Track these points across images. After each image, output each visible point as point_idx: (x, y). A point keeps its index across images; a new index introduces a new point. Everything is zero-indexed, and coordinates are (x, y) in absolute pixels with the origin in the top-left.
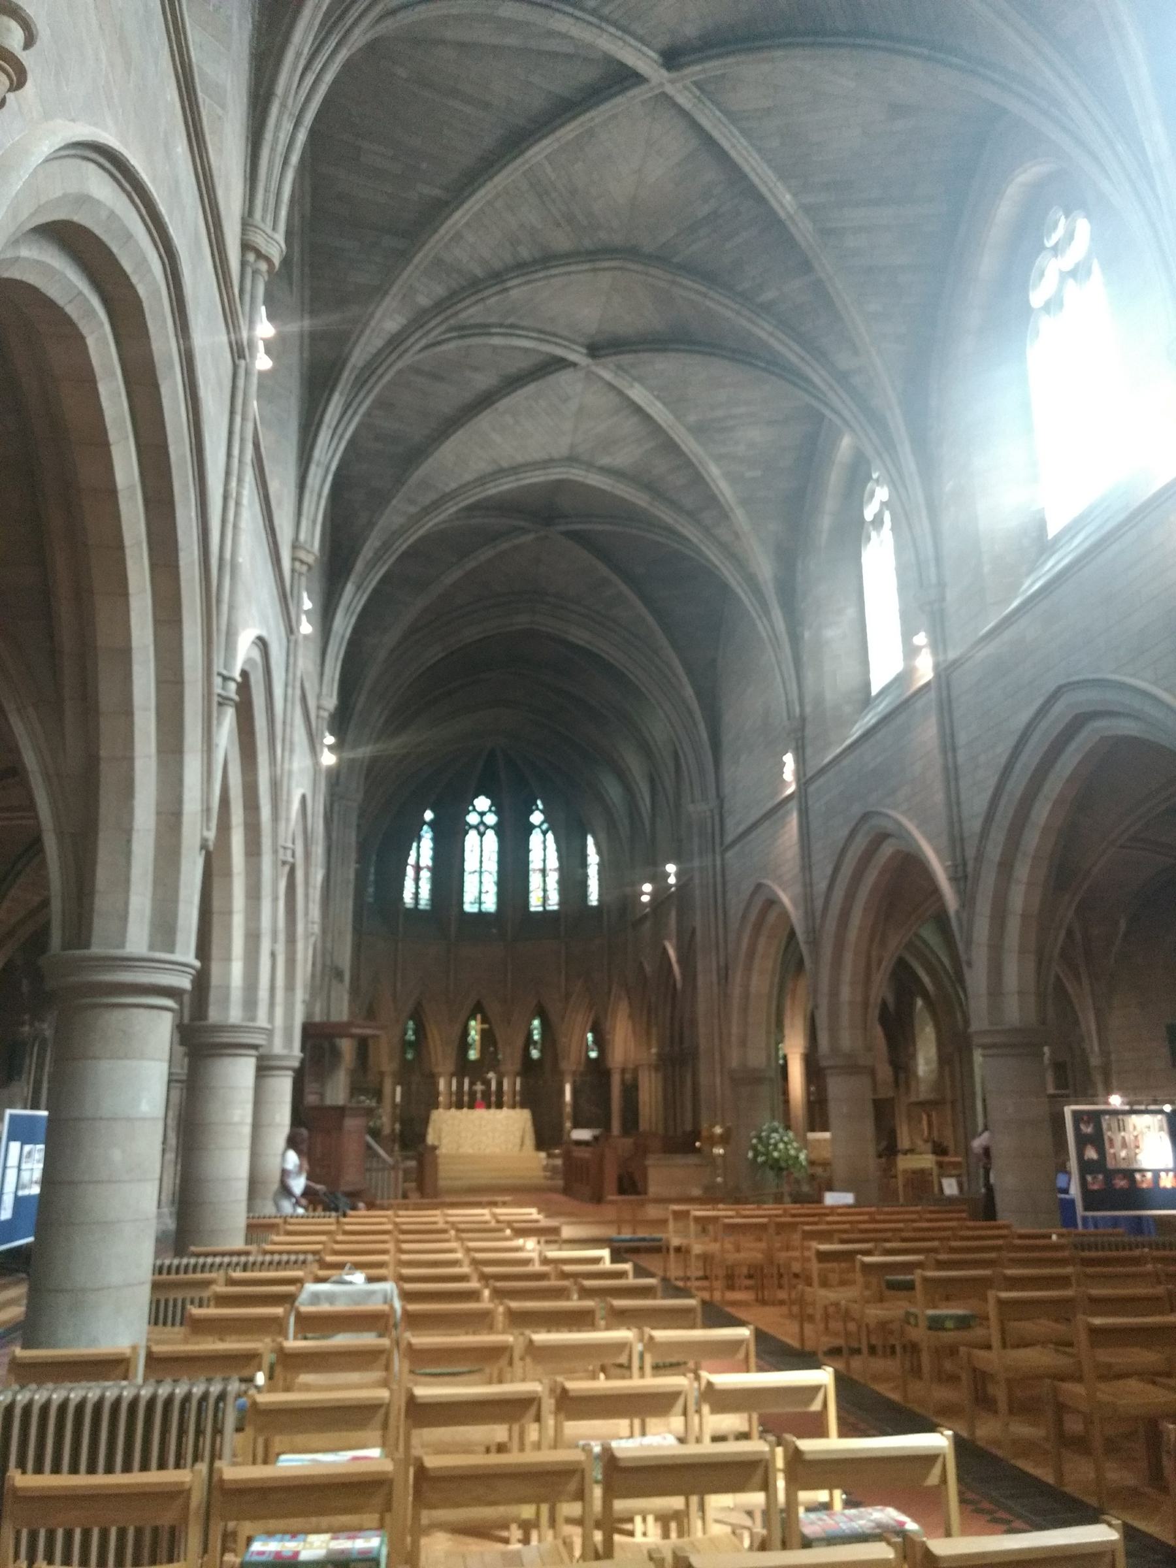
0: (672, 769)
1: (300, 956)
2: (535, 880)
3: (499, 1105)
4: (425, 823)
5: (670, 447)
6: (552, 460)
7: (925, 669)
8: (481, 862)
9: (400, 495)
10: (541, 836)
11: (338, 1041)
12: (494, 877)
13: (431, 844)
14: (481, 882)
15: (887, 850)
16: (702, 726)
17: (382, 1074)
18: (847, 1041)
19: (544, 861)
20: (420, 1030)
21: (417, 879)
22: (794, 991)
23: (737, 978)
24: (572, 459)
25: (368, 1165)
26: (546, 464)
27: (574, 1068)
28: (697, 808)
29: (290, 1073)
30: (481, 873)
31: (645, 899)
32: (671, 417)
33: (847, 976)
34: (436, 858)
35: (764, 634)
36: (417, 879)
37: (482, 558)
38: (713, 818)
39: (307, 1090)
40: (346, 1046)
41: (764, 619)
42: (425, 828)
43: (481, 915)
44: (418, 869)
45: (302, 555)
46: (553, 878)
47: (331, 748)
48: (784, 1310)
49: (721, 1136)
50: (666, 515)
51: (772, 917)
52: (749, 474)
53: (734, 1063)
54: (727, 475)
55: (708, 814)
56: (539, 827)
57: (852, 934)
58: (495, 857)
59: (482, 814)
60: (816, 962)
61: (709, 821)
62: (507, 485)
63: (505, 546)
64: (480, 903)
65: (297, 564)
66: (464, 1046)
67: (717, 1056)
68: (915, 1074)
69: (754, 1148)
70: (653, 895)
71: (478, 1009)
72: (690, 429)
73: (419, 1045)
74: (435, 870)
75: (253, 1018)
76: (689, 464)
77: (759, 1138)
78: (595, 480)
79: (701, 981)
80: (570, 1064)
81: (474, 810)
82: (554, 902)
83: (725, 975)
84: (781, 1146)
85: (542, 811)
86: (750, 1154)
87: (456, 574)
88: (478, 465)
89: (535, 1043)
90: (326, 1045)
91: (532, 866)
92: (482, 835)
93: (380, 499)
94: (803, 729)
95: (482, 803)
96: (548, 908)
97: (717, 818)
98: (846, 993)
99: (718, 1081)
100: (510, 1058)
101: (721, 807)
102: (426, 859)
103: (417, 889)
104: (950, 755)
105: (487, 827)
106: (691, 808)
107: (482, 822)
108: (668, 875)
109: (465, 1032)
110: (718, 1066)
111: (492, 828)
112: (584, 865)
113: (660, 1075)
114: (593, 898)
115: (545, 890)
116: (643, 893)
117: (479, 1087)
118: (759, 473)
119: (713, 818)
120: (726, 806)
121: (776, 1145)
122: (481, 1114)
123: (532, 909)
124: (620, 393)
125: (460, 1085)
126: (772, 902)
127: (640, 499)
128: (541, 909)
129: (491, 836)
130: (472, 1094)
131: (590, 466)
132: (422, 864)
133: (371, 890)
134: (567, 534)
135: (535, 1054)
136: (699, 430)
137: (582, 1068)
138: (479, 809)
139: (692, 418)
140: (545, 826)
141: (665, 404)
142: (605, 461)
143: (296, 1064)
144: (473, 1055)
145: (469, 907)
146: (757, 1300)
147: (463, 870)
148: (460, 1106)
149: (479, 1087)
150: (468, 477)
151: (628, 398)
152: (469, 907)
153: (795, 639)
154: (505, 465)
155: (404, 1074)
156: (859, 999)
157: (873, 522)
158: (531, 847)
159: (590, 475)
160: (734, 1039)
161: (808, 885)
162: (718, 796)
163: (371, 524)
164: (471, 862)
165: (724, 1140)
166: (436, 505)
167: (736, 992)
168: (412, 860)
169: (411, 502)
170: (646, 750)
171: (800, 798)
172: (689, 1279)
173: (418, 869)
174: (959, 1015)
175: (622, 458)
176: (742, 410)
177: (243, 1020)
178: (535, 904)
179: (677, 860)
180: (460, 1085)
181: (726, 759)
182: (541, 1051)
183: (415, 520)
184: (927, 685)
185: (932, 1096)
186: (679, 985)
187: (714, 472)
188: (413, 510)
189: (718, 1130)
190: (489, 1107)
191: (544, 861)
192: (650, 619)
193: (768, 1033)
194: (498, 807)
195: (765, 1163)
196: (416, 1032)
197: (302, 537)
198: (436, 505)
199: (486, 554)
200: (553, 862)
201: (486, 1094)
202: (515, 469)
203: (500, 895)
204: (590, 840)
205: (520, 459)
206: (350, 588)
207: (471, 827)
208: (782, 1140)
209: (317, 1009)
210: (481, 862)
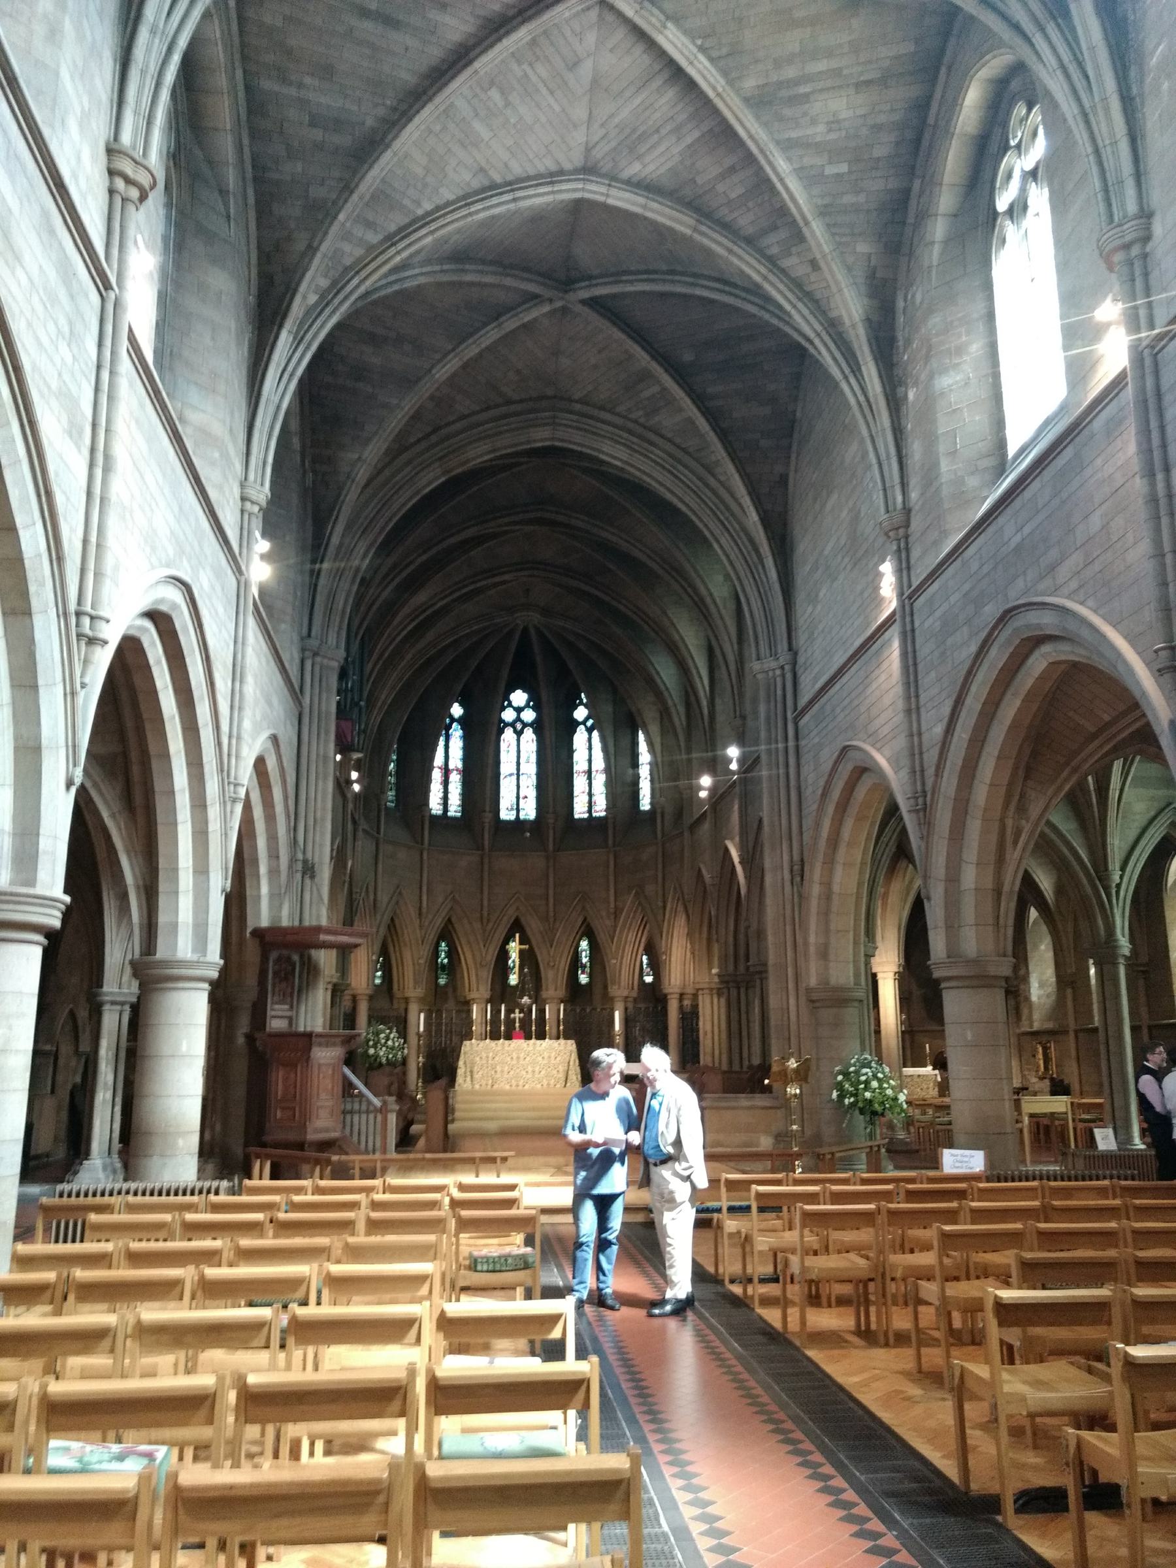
0: (733, 630)
1: (214, 826)
2: (580, 784)
3: (541, 1036)
4: (453, 720)
5: (724, 134)
6: (561, 172)
7: (1114, 354)
8: (518, 764)
9: (349, 206)
10: (586, 735)
11: (314, 953)
12: (533, 780)
13: (460, 744)
15: (1038, 663)
16: (769, 562)
17: (407, 1000)
18: (971, 942)
19: (590, 761)
20: (452, 953)
21: (446, 783)
22: (885, 896)
23: (816, 873)
24: (588, 170)
25: (349, 1107)
26: (554, 176)
27: (626, 993)
28: (763, 667)
29: (206, 986)
31: (703, 794)
32: (722, 81)
33: (971, 854)
34: (466, 759)
35: (852, 401)
36: (446, 783)
37: (486, 342)
38: (783, 676)
39: (270, 1013)
40: (326, 960)
41: (853, 381)
42: (455, 725)
43: (518, 823)
44: (446, 772)
45: (128, 168)
46: (599, 781)
47: (263, 557)
48: (903, 1358)
49: (797, 1071)
50: (716, 243)
51: (861, 792)
52: (830, 170)
53: (813, 982)
54: (799, 172)
55: (778, 672)
56: (584, 723)
57: (980, 794)
59: (519, 710)
60: (926, 838)
61: (779, 680)
62: (500, 206)
63: (510, 324)
64: (518, 810)
65: (120, 184)
67: (790, 971)
68: (1027, 999)
69: (839, 1086)
70: (713, 790)
71: (516, 927)
72: (746, 100)
73: (452, 968)
75: (32, 882)
76: (750, 159)
77: (846, 1074)
78: (622, 199)
79: (768, 879)
80: (622, 989)
81: (510, 705)
82: (600, 807)
83: (799, 872)
84: (875, 1084)
85: (586, 706)
86: (835, 1094)
87: (452, 365)
88: (461, 177)
90: (296, 958)
91: (576, 768)
92: (519, 734)
93: (321, 214)
94: (907, 525)
95: (519, 697)
97: (789, 676)
98: (969, 877)
99: (792, 1001)
100: (554, 986)
101: (794, 663)
102: (456, 761)
103: (445, 794)
104: (1160, 477)
105: (525, 725)
106: (756, 666)
107: (518, 719)
108: (730, 761)
109: (504, 955)
110: (791, 986)
111: (531, 725)
112: (635, 765)
113: (723, 1000)
114: (645, 804)
115: (590, 795)
116: (700, 788)
118: (843, 168)
119: (783, 676)
120: (801, 660)
121: (867, 1082)
122: (519, 1045)
123: (576, 816)
124: (651, 44)
126: (863, 770)
127: (680, 222)
128: (586, 816)
129: (529, 735)
130: (510, 1023)
131: (613, 178)
132: (451, 766)
133: (391, 794)
134: (594, 303)
135: (584, 979)
136: (759, 102)
137: (634, 994)
138: (515, 704)
139: (750, 83)
140: (590, 723)
141: (711, 60)
142: (634, 169)
143: (214, 974)
144: (513, 980)
145: (506, 814)
146: (858, 1333)
147: (499, 774)
148: (495, 1036)
149: (517, 1015)
150: (447, 195)
151: (662, 53)
152: (506, 814)
153: (895, 404)
154: (498, 179)
156: (989, 883)
157: (1010, 212)
159: (613, 192)
160: (812, 949)
161: (915, 735)
162: (790, 649)
163: (311, 250)
164: (507, 765)
165: (801, 1076)
166: (403, 232)
167: (816, 890)
168: (439, 760)
169: (370, 225)
170: (702, 610)
171: (903, 617)
172: (750, 1281)
173: (446, 772)
174: (1100, 922)
175: (656, 162)
176: (822, 66)
177: (12, 883)
178: (580, 810)
179: (741, 741)
181: (800, 597)
182: (591, 976)
183: (374, 252)
184: (1118, 383)
185: (1050, 1025)
186: (743, 891)
187: (782, 168)
188: (373, 238)
189: (793, 1064)
191: (590, 761)
192: (702, 424)
193: (856, 943)
194: (535, 702)
195: (852, 1105)
197: (126, 138)
198: (403, 232)
199: (490, 335)
200: (599, 763)
201: (525, 1022)
202: (511, 185)
204: (641, 737)
205: (517, 170)
206: (285, 339)
207: (507, 725)
208: (875, 1077)
209: (285, 912)
210: (518, 764)
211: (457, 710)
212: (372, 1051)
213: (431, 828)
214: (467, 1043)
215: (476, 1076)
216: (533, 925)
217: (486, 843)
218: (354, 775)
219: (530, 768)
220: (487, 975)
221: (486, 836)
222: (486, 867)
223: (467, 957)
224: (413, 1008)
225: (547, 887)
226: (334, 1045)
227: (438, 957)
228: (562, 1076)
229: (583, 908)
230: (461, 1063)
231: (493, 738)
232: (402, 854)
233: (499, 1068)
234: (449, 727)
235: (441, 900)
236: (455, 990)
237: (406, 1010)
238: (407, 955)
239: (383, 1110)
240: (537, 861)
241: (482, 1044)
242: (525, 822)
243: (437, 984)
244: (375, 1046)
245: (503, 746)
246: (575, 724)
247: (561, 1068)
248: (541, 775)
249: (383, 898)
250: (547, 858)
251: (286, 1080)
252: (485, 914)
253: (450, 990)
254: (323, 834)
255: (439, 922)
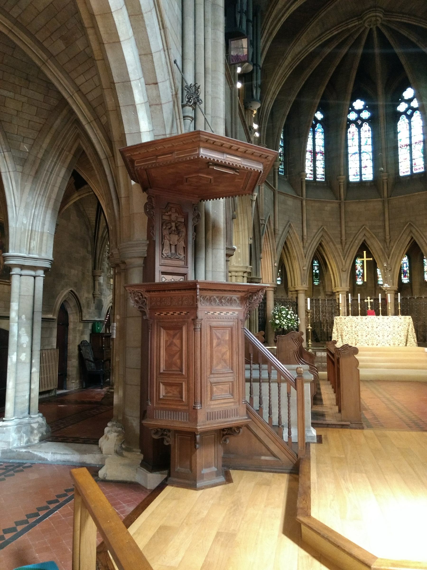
3: (385, 313)
8: (360, 146)
10: (407, 121)
12: (370, 156)
13: (322, 136)
14: (360, 161)
19: (410, 138)
21: (314, 161)
30: (360, 153)
36: (314, 161)
42: (318, 125)
43: (362, 184)
44: (314, 153)
58: (370, 141)
59: (359, 112)
64: (361, 175)
66: (353, 276)
74: (327, 154)
81: (353, 110)
89: (405, 273)
91: (400, 144)
92: (359, 127)
95: (359, 104)
96: (415, 172)
105: (363, 121)
107: (359, 118)
117: (369, 300)
122: (371, 319)
123: (401, 174)
125: (355, 300)
128: (409, 173)
129: (366, 127)
130: (364, 305)
132: (318, 149)
138: (356, 108)
144: (359, 282)
145: (353, 178)
147: (347, 154)
148: (355, 314)
152: (353, 178)
155: (313, 292)
158: (398, 131)
164: (353, 149)
168: (309, 147)
173: (314, 153)
178: (404, 170)
180: (355, 300)
182: (410, 278)
190: (378, 314)
191: (410, 138)
196: (319, 268)
201: (375, 306)
203: (375, 168)
210: (360, 146)
211: (319, 116)
212: (277, 322)
213: (307, 186)
214: (338, 317)
215: (344, 338)
216: (375, 245)
217: (342, 197)
218: (255, 126)
219: (368, 148)
220: (346, 276)
221: (342, 190)
222: (343, 211)
223: (333, 266)
224: (301, 297)
225: (384, 221)
226: (230, 301)
227: (313, 269)
228: (403, 339)
229: (411, 231)
230: (334, 330)
231: (344, 132)
232: (290, 202)
233: (359, 334)
234: (314, 127)
235: (315, 231)
236: (324, 288)
237: (297, 298)
238: (296, 266)
239: (296, 383)
240: (375, 205)
241: (348, 318)
242: (366, 182)
243: (313, 285)
244: (279, 318)
245: (349, 136)
246: (397, 116)
247: (404, 333)
248: (375, 152)
249: (280, 228)
250: (383, 202)
251: (169, 346)
252: (344, 238)
253: (321, 288)
254: (215, 86)
255: (315, 245)
